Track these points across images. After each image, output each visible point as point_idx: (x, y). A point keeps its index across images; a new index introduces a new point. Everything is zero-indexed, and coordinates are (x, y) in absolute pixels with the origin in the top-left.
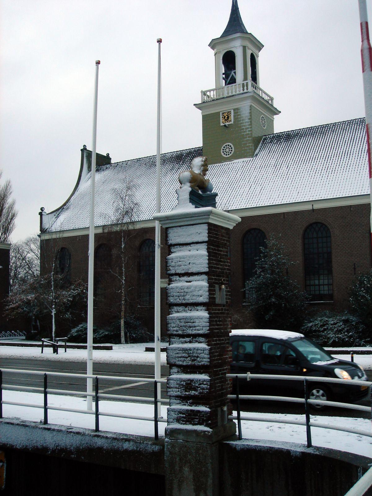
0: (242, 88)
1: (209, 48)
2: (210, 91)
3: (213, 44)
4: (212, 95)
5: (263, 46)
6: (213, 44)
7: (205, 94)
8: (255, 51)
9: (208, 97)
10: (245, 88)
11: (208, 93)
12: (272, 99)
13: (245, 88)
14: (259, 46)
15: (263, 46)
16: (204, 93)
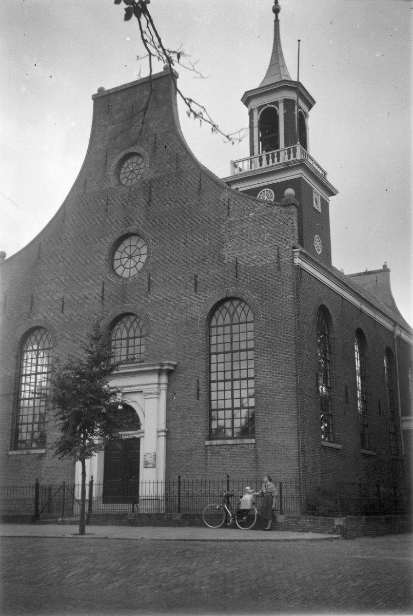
0: (287, 156)
1: (242, 103)
2: (243, 160)
3: (247, 99)
4: (245, 166)
5: (315, 102)
6: (247, 99)
7: (235, 166)
8: (304, 107)
9: (240, 170)
10: (292, 155)
11: (240, 165)
12: (325, 174)
13: (292, 155)
14: (310, 103)
15: (315, 102)
16: (235, 165)
